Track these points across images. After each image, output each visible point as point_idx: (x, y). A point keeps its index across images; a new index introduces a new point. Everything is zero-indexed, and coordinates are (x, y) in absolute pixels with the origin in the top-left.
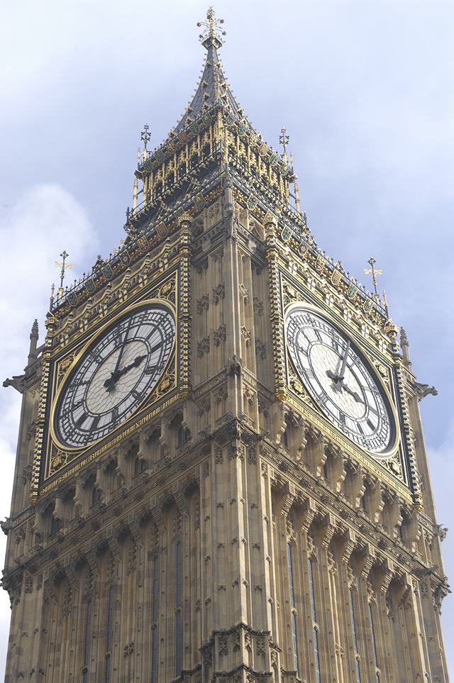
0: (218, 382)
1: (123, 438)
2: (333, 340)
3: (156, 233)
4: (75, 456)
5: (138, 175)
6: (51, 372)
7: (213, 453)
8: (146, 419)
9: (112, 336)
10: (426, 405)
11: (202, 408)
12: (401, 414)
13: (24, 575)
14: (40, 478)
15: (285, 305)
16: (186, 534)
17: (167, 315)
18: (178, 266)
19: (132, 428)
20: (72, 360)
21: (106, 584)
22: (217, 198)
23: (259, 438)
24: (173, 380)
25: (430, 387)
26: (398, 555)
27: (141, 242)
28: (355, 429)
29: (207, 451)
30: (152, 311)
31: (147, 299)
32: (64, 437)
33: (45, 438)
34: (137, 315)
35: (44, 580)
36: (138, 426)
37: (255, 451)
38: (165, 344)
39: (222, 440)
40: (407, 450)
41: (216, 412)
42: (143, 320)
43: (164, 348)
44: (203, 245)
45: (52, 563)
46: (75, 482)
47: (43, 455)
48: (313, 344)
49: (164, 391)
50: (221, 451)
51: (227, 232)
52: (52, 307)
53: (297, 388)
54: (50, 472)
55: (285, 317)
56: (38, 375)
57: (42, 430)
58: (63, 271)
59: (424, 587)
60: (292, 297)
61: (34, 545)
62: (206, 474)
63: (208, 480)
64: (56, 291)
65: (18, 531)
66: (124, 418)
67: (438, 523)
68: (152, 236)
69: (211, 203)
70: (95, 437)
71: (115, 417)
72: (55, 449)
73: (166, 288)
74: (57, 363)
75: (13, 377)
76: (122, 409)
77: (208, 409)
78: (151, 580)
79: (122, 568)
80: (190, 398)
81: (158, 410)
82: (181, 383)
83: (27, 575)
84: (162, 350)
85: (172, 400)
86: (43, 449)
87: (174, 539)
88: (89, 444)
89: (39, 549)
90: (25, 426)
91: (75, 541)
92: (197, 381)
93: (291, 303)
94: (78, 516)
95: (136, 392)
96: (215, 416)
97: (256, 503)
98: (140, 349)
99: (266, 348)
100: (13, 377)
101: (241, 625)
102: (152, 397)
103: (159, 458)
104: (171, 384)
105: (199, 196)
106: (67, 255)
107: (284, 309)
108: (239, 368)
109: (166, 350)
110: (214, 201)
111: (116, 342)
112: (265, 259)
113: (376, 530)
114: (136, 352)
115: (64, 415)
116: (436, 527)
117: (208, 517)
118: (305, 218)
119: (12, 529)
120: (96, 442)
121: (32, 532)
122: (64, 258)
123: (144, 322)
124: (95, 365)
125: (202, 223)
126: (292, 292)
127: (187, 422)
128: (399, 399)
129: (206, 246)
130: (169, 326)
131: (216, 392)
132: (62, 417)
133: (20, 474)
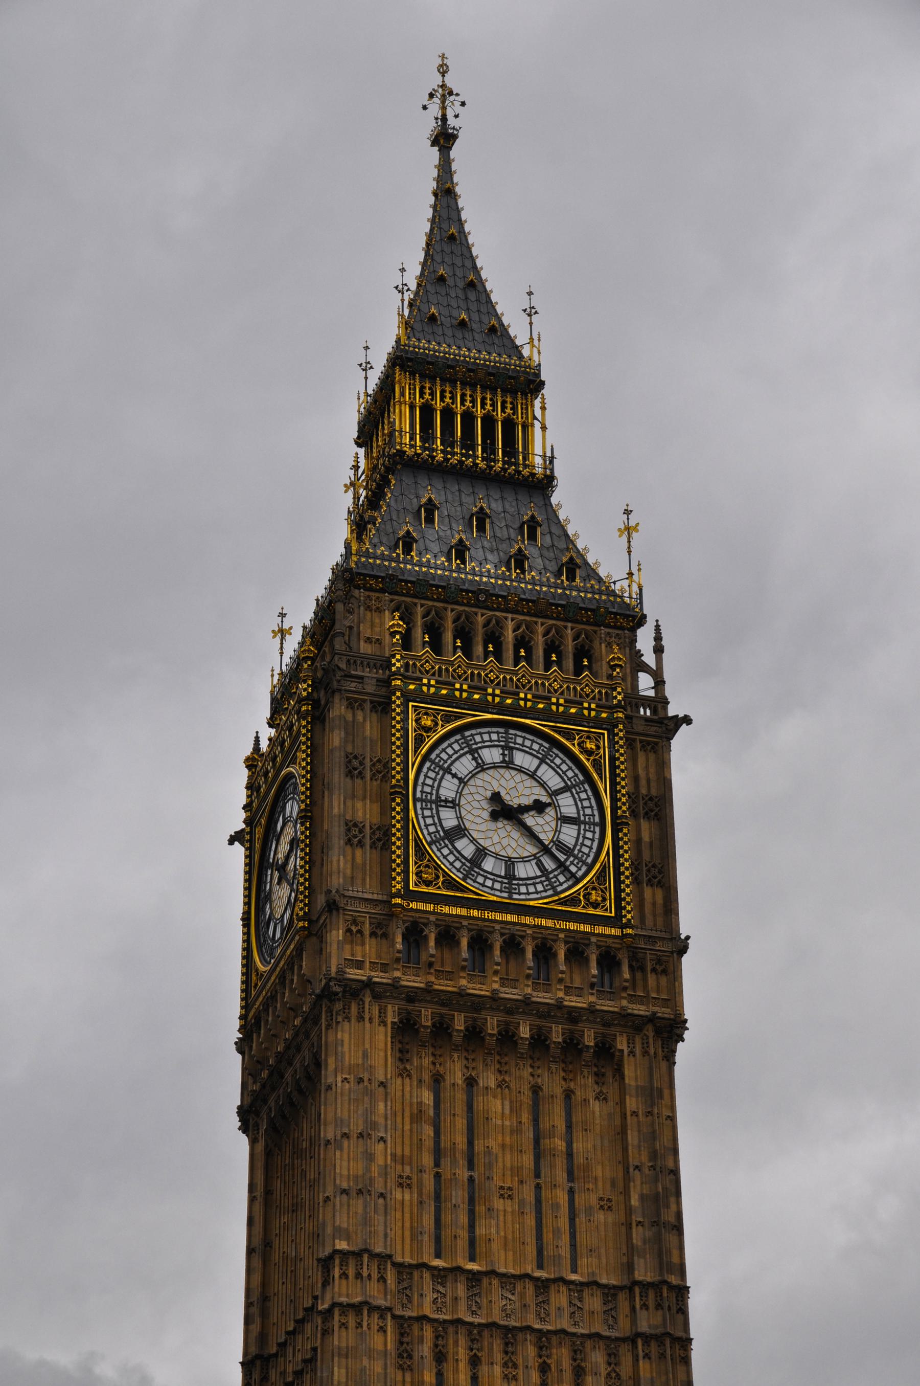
5: (359, 445)
12: (614, 800)
23: (369, 984)
25: (681, 715)
55: (412, 776)
60: (428, 729)
80: (310, 935)
91: (273, 1089)
101: (336, 1252)
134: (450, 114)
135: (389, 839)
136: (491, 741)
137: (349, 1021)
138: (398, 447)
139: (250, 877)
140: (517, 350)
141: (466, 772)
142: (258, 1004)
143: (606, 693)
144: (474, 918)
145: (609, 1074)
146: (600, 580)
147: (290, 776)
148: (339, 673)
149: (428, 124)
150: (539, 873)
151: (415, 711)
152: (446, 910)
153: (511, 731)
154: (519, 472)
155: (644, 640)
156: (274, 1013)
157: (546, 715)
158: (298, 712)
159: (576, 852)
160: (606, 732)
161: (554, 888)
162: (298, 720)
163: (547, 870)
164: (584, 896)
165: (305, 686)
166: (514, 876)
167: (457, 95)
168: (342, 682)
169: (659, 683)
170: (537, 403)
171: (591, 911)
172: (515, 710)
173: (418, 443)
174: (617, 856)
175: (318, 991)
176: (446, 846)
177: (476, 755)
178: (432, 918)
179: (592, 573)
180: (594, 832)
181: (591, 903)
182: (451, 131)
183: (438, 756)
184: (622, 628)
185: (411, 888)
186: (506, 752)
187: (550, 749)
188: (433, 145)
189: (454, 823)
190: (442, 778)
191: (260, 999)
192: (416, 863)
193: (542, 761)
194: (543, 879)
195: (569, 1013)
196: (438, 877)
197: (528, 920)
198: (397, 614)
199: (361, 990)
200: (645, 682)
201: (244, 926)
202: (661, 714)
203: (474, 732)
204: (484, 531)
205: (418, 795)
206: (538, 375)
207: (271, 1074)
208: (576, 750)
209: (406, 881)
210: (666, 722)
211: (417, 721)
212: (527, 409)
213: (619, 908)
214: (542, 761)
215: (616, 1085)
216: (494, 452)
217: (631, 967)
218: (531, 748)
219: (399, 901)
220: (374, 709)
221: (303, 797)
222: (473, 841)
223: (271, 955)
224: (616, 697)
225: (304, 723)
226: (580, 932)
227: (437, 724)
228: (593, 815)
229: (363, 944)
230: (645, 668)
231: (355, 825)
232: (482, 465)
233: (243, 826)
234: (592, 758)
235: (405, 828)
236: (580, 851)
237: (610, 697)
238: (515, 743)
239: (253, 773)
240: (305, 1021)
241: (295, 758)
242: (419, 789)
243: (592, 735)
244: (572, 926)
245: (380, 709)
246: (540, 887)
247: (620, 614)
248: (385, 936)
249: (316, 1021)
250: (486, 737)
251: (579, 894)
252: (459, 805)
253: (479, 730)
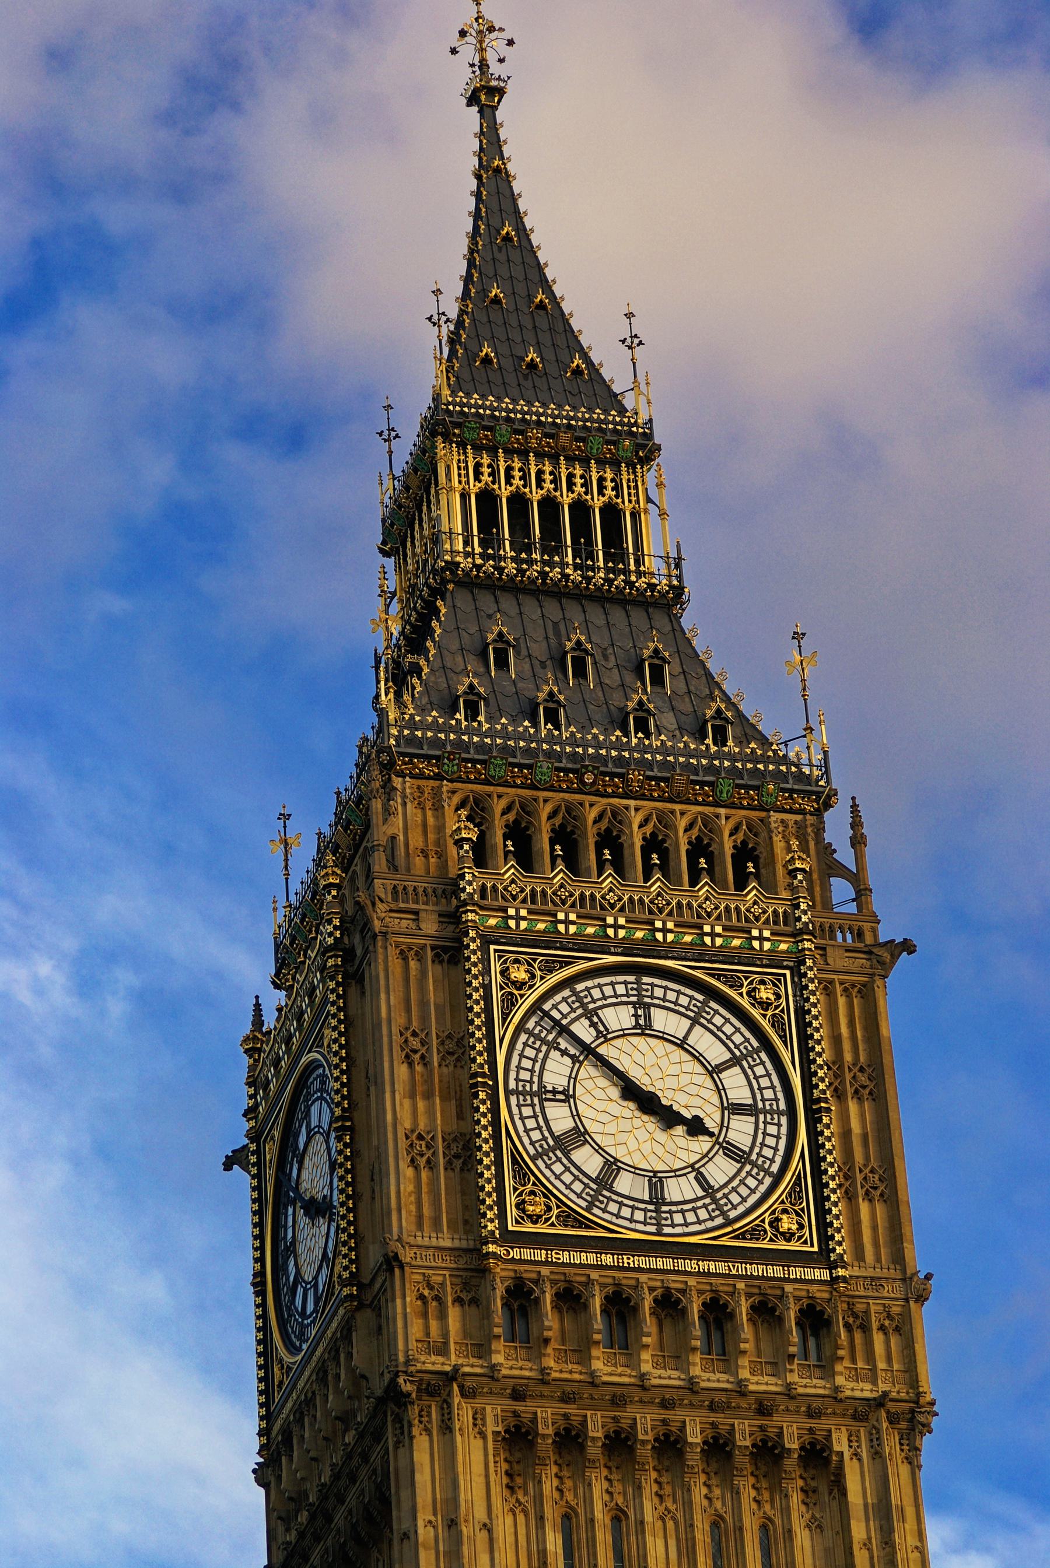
5: (386, 554)
12: (807, 1076)
15: (504, 1020)
40: (817, 1160)
60: (520, 985)
80: (361, 1306)
126: (519, 974)
134: (491, 57)
135: (472, 1156)
138: (448, 558)
139: (261, 1218)
140: (614, 401)
142: (285, 1411)
143: (785, 912)
144: (607, 1267)
145: (823, 1489)
146: (765, 742)
147: (313, 1066)
149: (461, 75)
151: (500, 957)
152: (564, 1257)
154: (631, 584)
155: (836, 827)
156: (312, 1425)
157: (699, 953)
158: (323, 969)
159: (754, 1157)
160: (788, 972)
161: (723, 1214)
162: (323, 980)
163: (712, 1187)
164: (771, 1224)
165: (330, 928)
166: (663, 1198)
167: (501, 30)
169: (862, 893)
170: (651, 477)
171: (782, 1245)
172: (650, 948)
173: (478, 550)
174: (817, 1160)
175: (379, 1392)
176: (559, 1160)
177: (595, 1019)
178: (545, 1271)
179: (749, 732)
180: (779, 1125)
181: (783, 1234)
182: (494, 83)
184: (801, 812)
185: (510, 1228)
186: (640, 1012)
187: (705, 1003)
188: (469, 104)
189: (569, 1124)
190: (546, 1056)
191: (289, 1404)
192: (515, 1189)
193: (695, 1021)
194: (708, 1201)
195: (760, 1404)
196: (549, 1209)
197: (690, 1265)
198: (464, 813)
200: (841, 889)
201: (257, 1294)
202: (869, 939)
204: (585, 676)
205: (512, 1085)
206: (648, 436)
207: (312, 1517)
208: (745, 1002)
209: (502, 1216)
210: (875, 950)
211: (504, 972)
212: (636, 487)
213: (825, 1238)
215: (835, 1504)
216: (591, 555)
217: (847, 1325)
218: (676, 1003)
219: (492, 1248)
220: (437, 958)
221: (337, 1098)
222: (599, 1149)
223: (302, 1337)
224: (799, 919)
225: (332, 985)
226: (768, 1279)
228: (777, 1100)
230: (840, 870)
232: (576, 576)
233: (246, 1141)
234: (769, 1013)
235: (496, 1137)
236: (759, 1155)
237: (791, 919)
239: (256, 1061)
240: (361, 1436)
241: (320, 1037)
242: (512, 1075)
243: (766, 978)
244: (756, 1270)
245: (446, 957)
247: (798, 791)
248: (475, 1301)
249: (378, 1436)
251: (763, 1221)
252: (574, 1096)
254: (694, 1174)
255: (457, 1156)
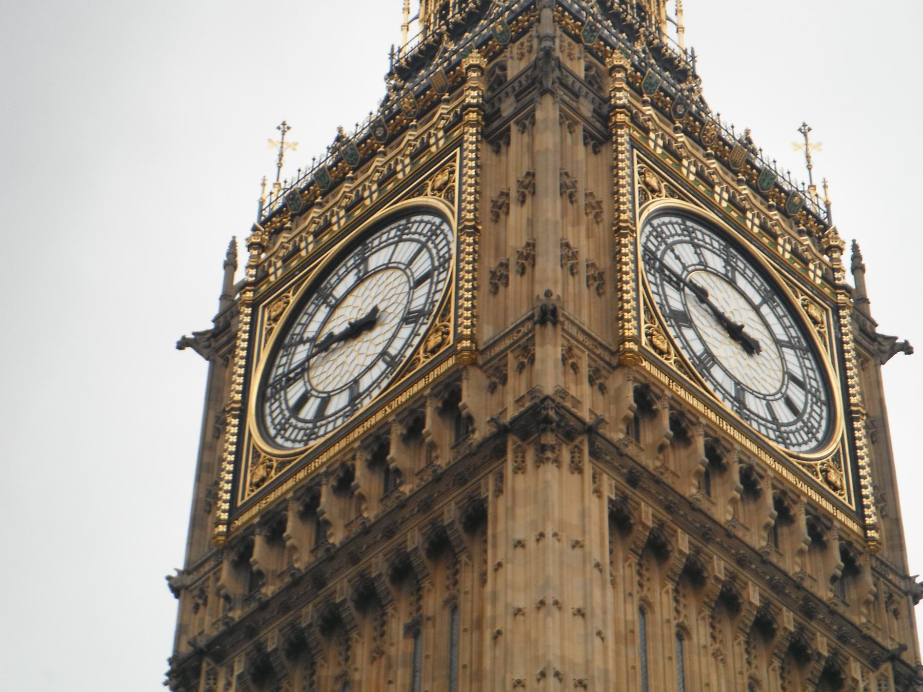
0: (520, 334)
1: (365, 432)
2: (725, 261)
3: (428, 87)
4: (288, 465)
6: (253, 324)
7: (510, 456)
8: (402, 398)
9: (352, 261)
10: (893, 372)
11: (494, 379)
12: (845, 387)
13: (204, 665)
14: (233, 501)
15: (640, 205)
16: (466, 593)
17: (441, 224)
18: (459, 142)
19: (380, 415)
20: (288, 303)
21: (337, 679)
22: (530, 26)
23: (591, 431)
24: (448, 333)
25: (900, 340)
26: (835, 627)
27: (407, 103)
28: (763, 412)
29: (500, 453)
30: (418, 218)
31: (409, 198)
32: (273, 432)
33: (240, 434)
34: (392, 226)
35: (236, 673)
36: (389, 410)
37: (581, 451)
38: (436, 273)
39: (524, 436)
40: (854, 449)
41: (516, 386)
42: (403, 234)
43: (435, 280)
44: (503, 106)
45: (249, 646)
46: (286, 509)
47: (237, 463)
48: (690, 269)
49: (433, 351)
50: (524, 453)
51: (541, 83)
52: (260, 214)
53: (658, 343)
54: (247, 492)
55: (639, 224)
56: (234, 329)
57: (235, 421)
58: (281, 155)
59: (883, 682)
60: (653, 191)
61: (221, 615)
62: (499, 491)
63: (501, 500)
64: (269, 188)
65: (196, 592)
66: (368, 398)
67: (912, 574)
68: (423, 92)
69: (520, 36)
70: (322, 432)
71: (355, 398)
72: (257, 455)
73: (441, 179)
74: (264, 307)
75: (194, 334)
76: (365, 383)
77: (504, 380)
78: (409, 671)
79: (361, 652)
80: (474, 363)
81: (421, 384)
82: (459, 338)
83: (209, 665)
84: (432, 283)
85: (443, 368)
86: (238, 454)
87: (446, 602)
88: (312, 443)
89: (227, 621)
90: (212, 415)
91: (285, 608)
92: (487, 333)
93: (651, 200)
94: (291, 567)
95: (389, 355)
96: (514, 390)
97: (580, 539)
98: (396, 283)
99: (607, 277)
100: (194, 334)
102: (412, 362)
103: (423, 464)
104: (443, 340)
105: (501, 23)
106: (289, 128)
107: (638, 211)
108: (554, 312)
109: (438, 282)
110: (525, 31)
111: (359, 271)
112: (607, 127)
113: (799, 587)
114: (390, 287)
115: (273, 396)
116: (906, 577)
117: (500, 565)
118: (693, 58)
119: (186, 588)
120: (322, 440)
121: (218, 593)
122: (284, 132)
123: (405, 237)
124: (323, 311)
125: (504, 68)
126: (653, 182)
127: (468, 404)
128: (843, 361)
129: (508, 107)
130: (444, 242)
131: (518, 352)
132: (269, 399)
133: (202, 495)
136: (711, 245)
137: (559, 466)
141: (690, 263)
144: (710, 420)
148: (557, 73)
150: (769, 418)
151: (638, 163)
152: (681, 392)
153: (731, 250)
168: (557, 85)
180: (822, 411)
183: (659, 226)
192: (646, 323)
193: (764, 301)
194: (775, 427)
196: (668, 353)
199: (580, 434)
203: (696, 226)
210: (880, 340)
214: (764, 301)
227: (660, 191)
229: (578, 382)
231: (567, 245)
238: (736, 263)
245: (592, 143)
246: (772, 435)
250: (707, 239)
253: (700, 228)
254: (764, 402)
255: (595, 279)
